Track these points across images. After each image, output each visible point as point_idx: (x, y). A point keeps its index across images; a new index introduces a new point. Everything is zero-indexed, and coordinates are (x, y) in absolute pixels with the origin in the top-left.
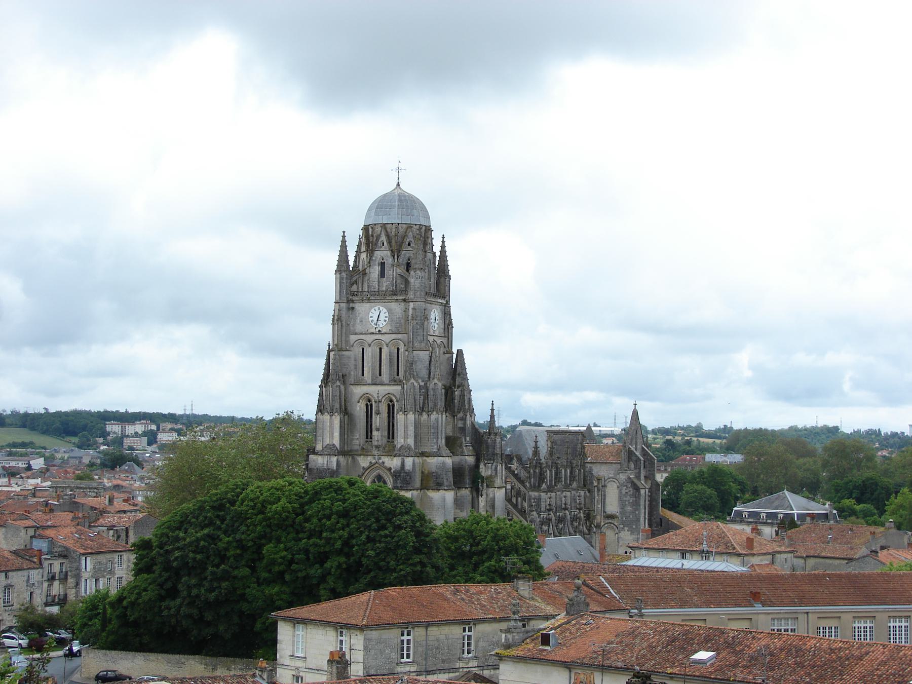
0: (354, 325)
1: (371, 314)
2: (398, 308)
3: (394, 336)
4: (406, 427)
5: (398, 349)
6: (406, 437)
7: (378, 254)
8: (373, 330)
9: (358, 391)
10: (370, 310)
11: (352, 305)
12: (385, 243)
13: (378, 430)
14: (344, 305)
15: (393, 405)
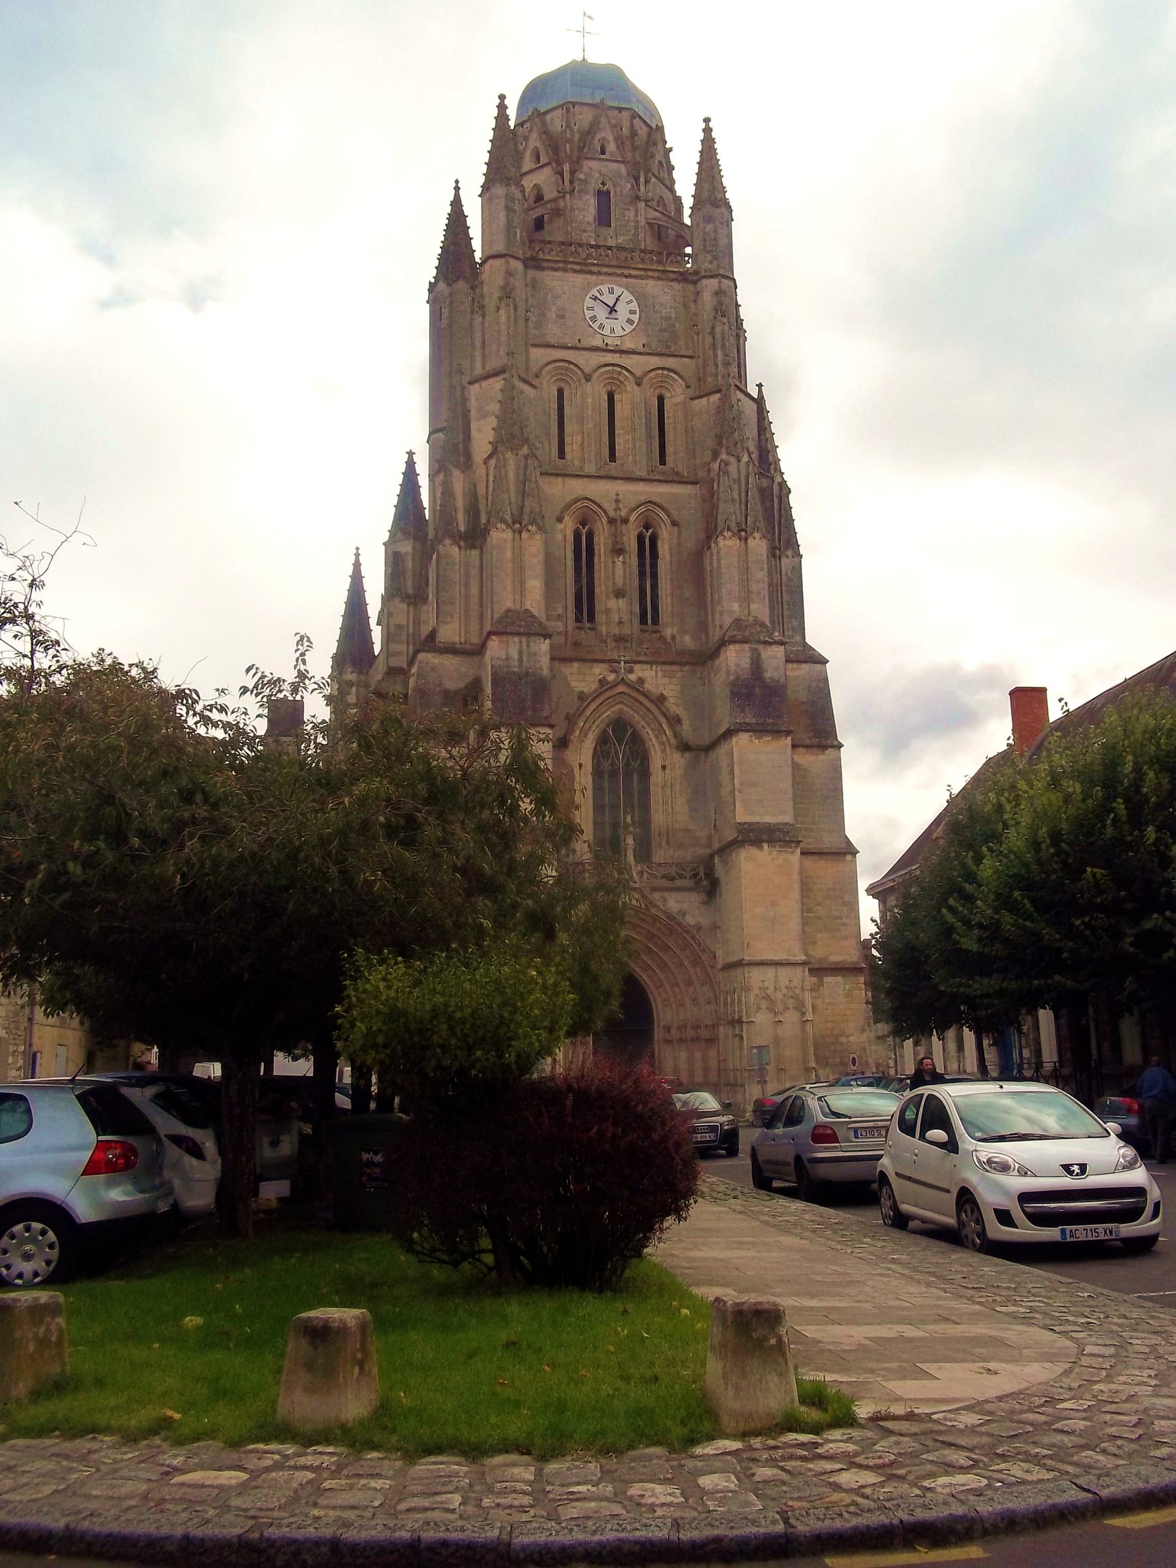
2: (664, 294)
3: (655, 361)
4: (745, 570)
5: (661, 400)
6: (746, 598)
7: (594, 170)
8: (598, 342)
9: (560, 491)
11: (531, 273)
12: (612, 147)
13: (619, 594)
14: (517, 265)
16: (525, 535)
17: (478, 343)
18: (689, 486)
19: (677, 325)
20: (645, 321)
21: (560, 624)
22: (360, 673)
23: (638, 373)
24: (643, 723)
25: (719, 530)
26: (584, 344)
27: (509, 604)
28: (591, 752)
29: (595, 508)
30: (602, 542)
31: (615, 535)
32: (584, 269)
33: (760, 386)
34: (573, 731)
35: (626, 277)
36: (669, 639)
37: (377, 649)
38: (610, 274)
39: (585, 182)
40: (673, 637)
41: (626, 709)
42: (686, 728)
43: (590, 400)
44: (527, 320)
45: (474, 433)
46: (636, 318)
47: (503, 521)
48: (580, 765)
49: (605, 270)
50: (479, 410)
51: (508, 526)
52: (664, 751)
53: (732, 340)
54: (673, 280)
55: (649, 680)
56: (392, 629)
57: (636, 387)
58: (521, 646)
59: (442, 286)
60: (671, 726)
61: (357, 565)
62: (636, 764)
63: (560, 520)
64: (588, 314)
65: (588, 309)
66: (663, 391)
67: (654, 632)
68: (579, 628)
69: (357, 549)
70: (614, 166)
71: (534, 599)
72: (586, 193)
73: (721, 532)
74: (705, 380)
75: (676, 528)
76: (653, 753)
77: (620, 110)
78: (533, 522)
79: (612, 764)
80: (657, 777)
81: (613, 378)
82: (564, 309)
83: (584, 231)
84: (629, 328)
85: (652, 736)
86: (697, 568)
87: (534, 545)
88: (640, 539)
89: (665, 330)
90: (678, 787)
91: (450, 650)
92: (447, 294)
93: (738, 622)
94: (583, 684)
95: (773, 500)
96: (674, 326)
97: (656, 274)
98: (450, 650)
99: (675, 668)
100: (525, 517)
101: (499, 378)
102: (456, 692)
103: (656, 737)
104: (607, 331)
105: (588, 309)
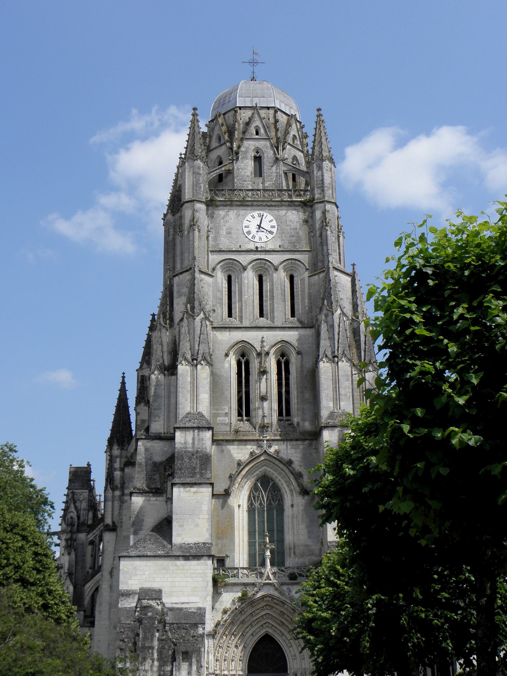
0: (215, 239)
1: (245, 223)
6: (337, 398)
8: (252, 246)
10: (244, 216)
12: (262, 131)
15: (287, 363)
16: (199, 367)
17: (178, 252)
18: (308, 330)
19: (301, 233)
20: (281, 231)
21: (227, 418)
22: (122, 449)
23: (276, 263)
24: (279, 478)
25: (320, 357)
26: (243, 248)
27: (188, 409)
28: (246, 498)
29: (248, 346)
30: (254, 366)
31: (260, 363)
32: (243, 204)
33: (354, 265)
34: (234, 484)
35: (269, 206)
36: (295, 425)
37: (134, 433)
38: (259, 206)
39: (246, 152)
40: (298, 423)
41: (269, 470)
42: (306, 481)
43: (246, 281)
44: (208, 237)
45: (175, 306)
46: (275, 230)
47: (186, 359)
48: (239, 506)
49: (255, 203)
50: (178, 292)
51: (189, 362)
52: (292, 495)
53: (334, 239)
54: (297, 206)
55: (282, 451)
56: (139, 423)
57: (274, 271)
58: (194, 435)
59: (169, 216)
60: (296, 479)
61: (123, 383)
62: (274, 504)
63: (227, 355)
64: (246, 230)
65: (246, 227)
66: (293, 273)
67: (287, 420)
68: (240, 421)
69: (124, 373)
70: (263, 143)
71: (204, 406)
72: (246, 158)
73: (322, 360)
74: (317, 265)
75: (300, 356)
76: (286, 497)
77: (268, 108)
78: (205, 359)
79: (261, 504)
80: (288, 511)
81: (261, 267)
82: (230, 228)
83: (245, 181)
84: (270, 236)
85: (285, 486)
86: (312, 379)
87: (204, 372)
88: (279, 363)
89: (293, 236)
90: (300, 517)
91: (159, 437)
92: (172, 221)
93: (332, 415)
94: (240, 455)
95: (359, 336)
96: (298, 233)
97: (287, 204)
98: (159, 437)
99: (299, 443)
100: (200, 356)
101: (188, 273)
102: (161, 463)
103: (288, 486)
104: (257, 239)
105: (246, 227)
